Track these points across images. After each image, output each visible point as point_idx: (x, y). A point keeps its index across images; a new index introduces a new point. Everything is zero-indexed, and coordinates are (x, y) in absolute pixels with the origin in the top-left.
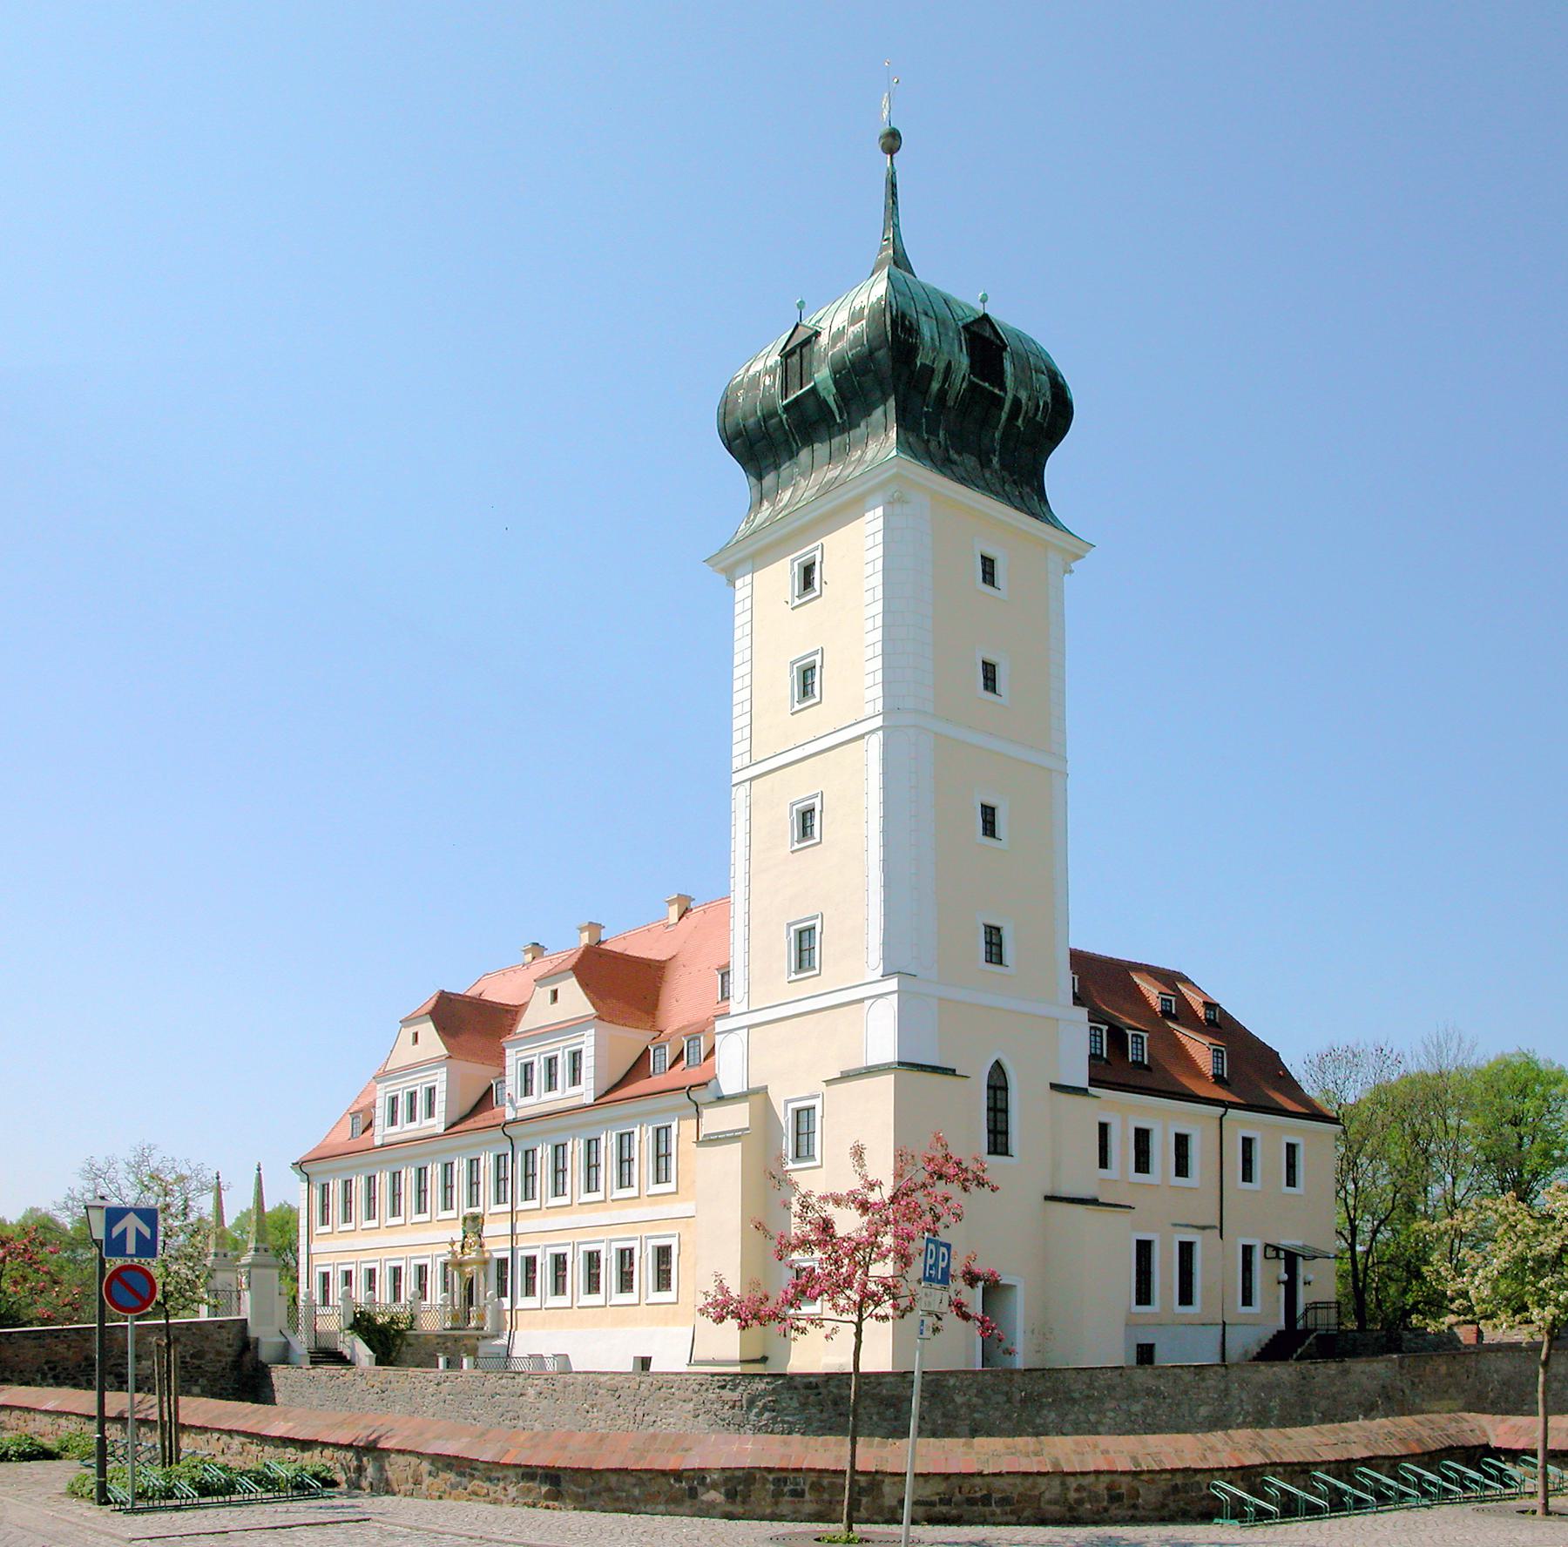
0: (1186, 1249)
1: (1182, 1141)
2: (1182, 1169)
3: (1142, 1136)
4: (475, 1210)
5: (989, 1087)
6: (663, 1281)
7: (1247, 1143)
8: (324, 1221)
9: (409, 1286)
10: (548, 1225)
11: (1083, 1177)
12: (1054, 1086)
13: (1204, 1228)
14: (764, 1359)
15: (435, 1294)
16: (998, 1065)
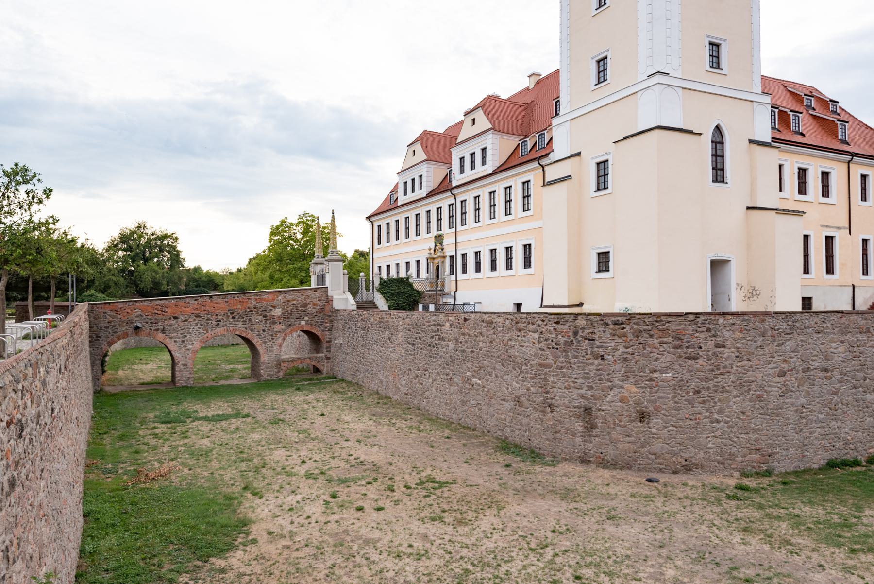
0: (829, 240)
1: (825, 175)
2: (826, 193)
3: (802, 173)
4: (440, 232)
6: (527, 263)
7: (864, 177)
8: (379, 243)
10: (474, 237)
12: (751, 141)
13: (839, 228)
14: (581, 304)
15: (424, 274)
16: (718, 128)
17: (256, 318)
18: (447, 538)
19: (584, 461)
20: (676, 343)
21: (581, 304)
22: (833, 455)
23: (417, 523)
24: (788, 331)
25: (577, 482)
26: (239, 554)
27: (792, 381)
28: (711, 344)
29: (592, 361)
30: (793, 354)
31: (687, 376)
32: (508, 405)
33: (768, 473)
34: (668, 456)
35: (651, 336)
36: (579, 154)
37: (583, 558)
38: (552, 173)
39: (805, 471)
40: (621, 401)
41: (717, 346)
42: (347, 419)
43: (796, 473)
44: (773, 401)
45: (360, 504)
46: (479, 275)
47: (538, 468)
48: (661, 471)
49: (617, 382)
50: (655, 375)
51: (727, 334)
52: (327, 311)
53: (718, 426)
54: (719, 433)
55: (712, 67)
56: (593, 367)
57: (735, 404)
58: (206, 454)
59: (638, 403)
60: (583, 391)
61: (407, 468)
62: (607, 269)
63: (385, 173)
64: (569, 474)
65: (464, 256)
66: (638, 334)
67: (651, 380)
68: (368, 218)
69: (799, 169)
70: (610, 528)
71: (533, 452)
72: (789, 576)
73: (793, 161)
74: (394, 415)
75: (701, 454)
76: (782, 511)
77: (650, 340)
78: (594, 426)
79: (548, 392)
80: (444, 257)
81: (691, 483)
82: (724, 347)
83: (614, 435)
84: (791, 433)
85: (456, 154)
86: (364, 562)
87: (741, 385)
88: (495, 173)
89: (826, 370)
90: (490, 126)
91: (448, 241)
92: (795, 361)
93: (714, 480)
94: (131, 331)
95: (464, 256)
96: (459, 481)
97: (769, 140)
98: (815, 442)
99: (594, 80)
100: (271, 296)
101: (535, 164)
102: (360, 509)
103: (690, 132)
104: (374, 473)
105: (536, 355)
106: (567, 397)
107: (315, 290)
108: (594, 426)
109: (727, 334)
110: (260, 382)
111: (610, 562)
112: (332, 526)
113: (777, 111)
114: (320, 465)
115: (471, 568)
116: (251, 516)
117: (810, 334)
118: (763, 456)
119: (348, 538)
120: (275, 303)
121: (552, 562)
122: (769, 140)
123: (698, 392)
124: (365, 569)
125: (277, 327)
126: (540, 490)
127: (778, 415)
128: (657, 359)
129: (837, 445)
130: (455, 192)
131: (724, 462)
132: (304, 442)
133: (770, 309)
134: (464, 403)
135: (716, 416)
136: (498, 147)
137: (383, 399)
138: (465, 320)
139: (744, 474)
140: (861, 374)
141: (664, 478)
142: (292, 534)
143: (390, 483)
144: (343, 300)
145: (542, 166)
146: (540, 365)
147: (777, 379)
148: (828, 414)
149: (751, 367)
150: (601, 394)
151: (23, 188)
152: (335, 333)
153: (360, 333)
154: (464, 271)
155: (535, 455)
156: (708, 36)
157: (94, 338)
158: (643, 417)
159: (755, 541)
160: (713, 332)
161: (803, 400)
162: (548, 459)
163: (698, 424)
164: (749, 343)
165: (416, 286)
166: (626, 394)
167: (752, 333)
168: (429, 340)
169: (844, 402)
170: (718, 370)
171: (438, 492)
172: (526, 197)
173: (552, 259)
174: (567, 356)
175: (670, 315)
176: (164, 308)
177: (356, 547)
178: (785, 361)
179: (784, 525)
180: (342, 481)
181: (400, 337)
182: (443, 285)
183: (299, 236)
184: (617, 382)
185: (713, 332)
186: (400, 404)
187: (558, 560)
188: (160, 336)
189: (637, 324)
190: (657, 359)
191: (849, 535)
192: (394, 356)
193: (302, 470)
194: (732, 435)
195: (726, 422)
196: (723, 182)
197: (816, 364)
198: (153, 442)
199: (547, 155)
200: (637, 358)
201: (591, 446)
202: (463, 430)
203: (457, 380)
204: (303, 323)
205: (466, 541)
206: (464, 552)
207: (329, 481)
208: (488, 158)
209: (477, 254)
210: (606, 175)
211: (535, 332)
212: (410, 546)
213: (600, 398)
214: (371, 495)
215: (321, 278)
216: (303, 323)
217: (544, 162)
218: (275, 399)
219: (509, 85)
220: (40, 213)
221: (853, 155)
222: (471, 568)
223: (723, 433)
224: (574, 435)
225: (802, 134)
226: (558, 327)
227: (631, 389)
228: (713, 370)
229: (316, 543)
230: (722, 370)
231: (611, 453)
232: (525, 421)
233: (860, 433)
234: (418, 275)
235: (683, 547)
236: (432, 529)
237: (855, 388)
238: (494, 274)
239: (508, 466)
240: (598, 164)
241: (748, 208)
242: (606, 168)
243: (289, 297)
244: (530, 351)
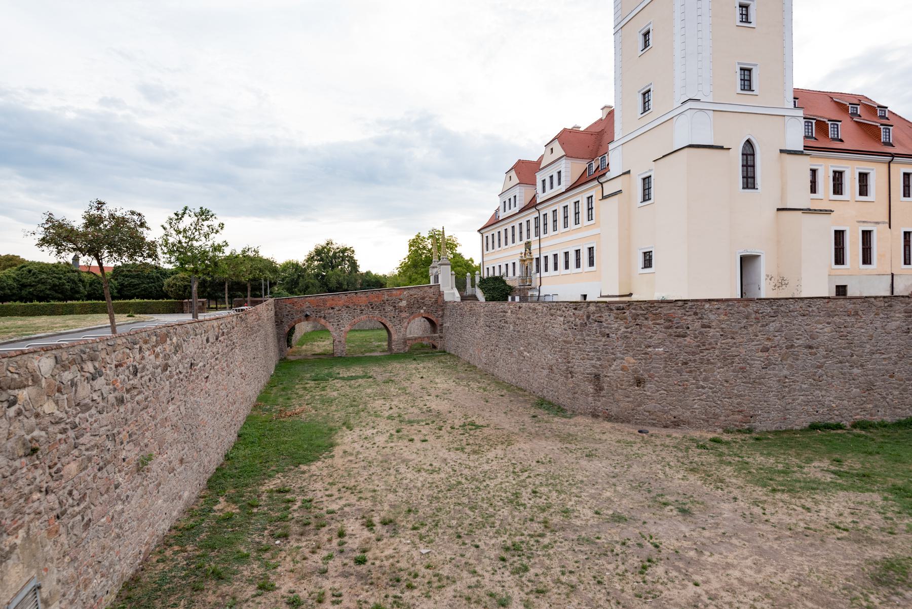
5: (743, 154)
6: (591, 263)
9: (503, 270)
10: (553, 243)
11: (801, 197)
12: (782, 151)
14: (631, 295)
15: (518, 273)
17: (389, 308)
18: (459, 461)
19: (595, 416)
20: (667, 324)
21: (631, 295)
22: (817, 419)
23: (444, 451)
24: (772, 314)
25: (581, 430)
26: (319, 463)
27: (775, 356)
28: (697, 325)
29: (600, 338)
30: (777, 334)
31: (677, 350)
32: (545, 372)
33: (750, 431)
34: (659, 414)
35: (646, 319)
36: (628, 172)
37: (547, 480)
38: (609, 189)
39: (785, 431)
40: (622, 369)
41: (704, 326)
42: (437, 380)
43: (776, 432)
44: (756, 372)
45: (413, 437)
46: (556, 273)
47: (556, 419)
48: (654, 425)
49: (619, 355)
50: (650, 350)
51: (712, 317)
52: (439, 303)
53: (703, 391)
54: (704, 397)
55: (744, 89)
56: (602, 343)
57: (719, 374)
58: (330, 401)
59: (635, 371)
60: (593, 362)
61: (459, 415)
62: (650, 266)
63: (489, 197)
64: (580, 424)
65: (546, 257)
66: (635, 317)
67: (646, 354)
68: (479, 231)
69: (835, 172)
70: (584, 463)
71: (559, 407)
72: (703, 503)
73: (826, 167)
74: (474, 380)
75: (688, 413)
76: (737, 459)
77: (645, 322)
78: (601, 389)
79: (569, 362)
80: (532, 259)
81: (674, 435)
82: (710, 327)
83: (617, 396)
84: (772, 398)
85: (539, 177)
86: (395, 472)
87: (725, 359)
88: (567, 191)
89: (811, 347)
90: (564, 153)
91: (534, 247)
92: (779, 339)
93: (696, 434)
94: (303, 317)
95: (546, 257)
96: (492, 426)
97: (802, 149)
98: (798, 407)
99: (641, 110)
100: (398, 292)
101: (595, 183)
102: (412, 440)
103: (722, 148)
104: (436, 419)
105: (562, 334)
106: (583, 366)
107: (431, 287)
108: (601, 389)
109: (712, 317)
110: (392, 355)
111: (566, 484)
112: (387, 450)
113: (814, 121)
114: (400, 411)
115: (463, 481)
116: (339, 441)
117: (795, 317)
118: (745, 416)
119: (393, 458)
120: (401, 297)
121: (524, 481)
122: (802, 149)
123: (686, 363)
124: (393, 477)
125: (404, 315)
126: (548, 434)
127: (760, 384)
128: (651, 337)
129: (821, 411)
130: (539, 207)
131: (709, 420)
132: (398, 395)
133: (796, 296)
134: (519, 370)
135: (701, 383)
136: (570, 170)
137: (471, 367)
138: (520, 308)
139: (727, 431)
140: (849, 351)
141: (652, 430)
142: (358, 453)
143: (442, 424)
144: (451, 294)
145: (602, 184)
146: (565, 342)
147: (760, 354)
148: (811, 384)
149: (735, 343)
150: (607, 364)
151: (206, 223)
152: (446, 319)
153: (459, 318)
154: (546, 270)
155: (559, 410)
156: (739, 63)
157: (279, 322)
158: (639, 382)
159: (692, 478)
160: (700, 315)
161: (785, 372)
162: (569, 413)
163: (686, 389)
164: (733, 324)
165: (509, 283)
166: (626, 365)
167: (736, 315)
168: (498, 323)
169: (829, 374)
170: (703, 345)
171: (472, 432)
172: (590, 209)
173: (607, 257)
174: (582, 335)
175: (663, 302)
176: (325, 301)
177: (394, 463)
178: (769, 339)
179: (729, 469)
180: (410, 422)
181: (481, 322)
182: (531, 281)
183: (430, 247)
184: (619, 355)
185: (700, 315)
186: (481, 371)
187: (528, 480)
188: (323, 321)
189: (635, 309)
190: (651, 337)
191: (781, 479)
192: (478, 335)
193: (386, 414)
194: (716, 399)
195: (711, 388)
196: (754, 188)
197: (800, 342)
198: (301, 392)
199: (604, 174)
200: (635, 336)
201: (599, 404)
202: (515, 390)
203: (515, 353)
204: (422, 311)
205: (472, 464)
206: (466, 472)
207: (401, 421)
208: (563, 179)
209: (555, 256)
210: (649, 188)
211: (561, 316)
212: (431, 465)
213: (606, 367)
214: (424, 432)
215: (436, 278)
216: (422, 311)
217: (602, 180)
218: (396, 366)
219: (585, 118)
220: (218, 239)
221: (893, 155)
222: (463, 481)
223: (708, 397)
224: (587, 395)
225: (841, 141)
226: (577, 312)
227: (630, 360)
228: (699, 346)
229: (370, 459)
230: (707, 346)
231: (614, 410)
232: (555, 384)
233: (845, 402)
234: (514, 274)
235: (632, 478)
236: (453, 455)
237: (841, 362)
238: (567, 271)
239: (534, 417)
240: (644, 179)
241: (779, 210)
242: (649, 183)
243: (412, 292)
244: (558, 330)
